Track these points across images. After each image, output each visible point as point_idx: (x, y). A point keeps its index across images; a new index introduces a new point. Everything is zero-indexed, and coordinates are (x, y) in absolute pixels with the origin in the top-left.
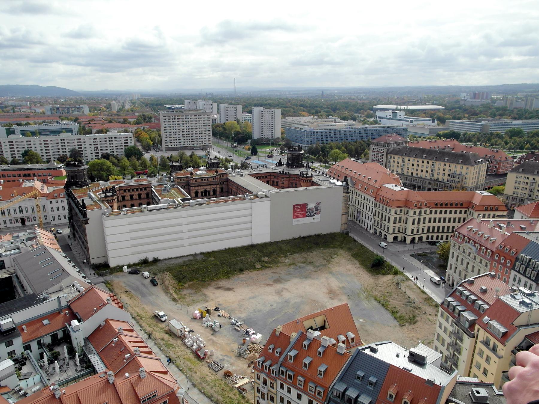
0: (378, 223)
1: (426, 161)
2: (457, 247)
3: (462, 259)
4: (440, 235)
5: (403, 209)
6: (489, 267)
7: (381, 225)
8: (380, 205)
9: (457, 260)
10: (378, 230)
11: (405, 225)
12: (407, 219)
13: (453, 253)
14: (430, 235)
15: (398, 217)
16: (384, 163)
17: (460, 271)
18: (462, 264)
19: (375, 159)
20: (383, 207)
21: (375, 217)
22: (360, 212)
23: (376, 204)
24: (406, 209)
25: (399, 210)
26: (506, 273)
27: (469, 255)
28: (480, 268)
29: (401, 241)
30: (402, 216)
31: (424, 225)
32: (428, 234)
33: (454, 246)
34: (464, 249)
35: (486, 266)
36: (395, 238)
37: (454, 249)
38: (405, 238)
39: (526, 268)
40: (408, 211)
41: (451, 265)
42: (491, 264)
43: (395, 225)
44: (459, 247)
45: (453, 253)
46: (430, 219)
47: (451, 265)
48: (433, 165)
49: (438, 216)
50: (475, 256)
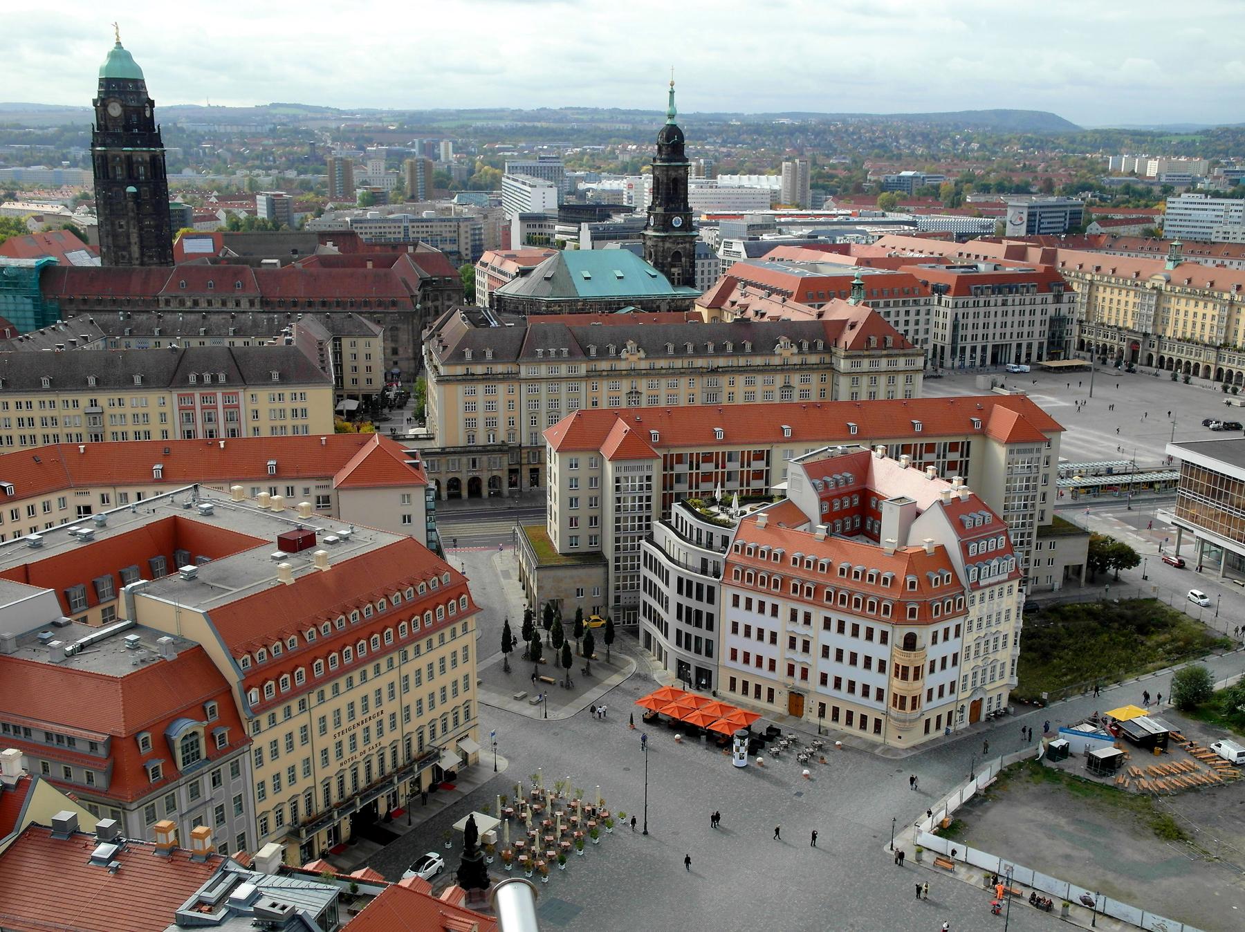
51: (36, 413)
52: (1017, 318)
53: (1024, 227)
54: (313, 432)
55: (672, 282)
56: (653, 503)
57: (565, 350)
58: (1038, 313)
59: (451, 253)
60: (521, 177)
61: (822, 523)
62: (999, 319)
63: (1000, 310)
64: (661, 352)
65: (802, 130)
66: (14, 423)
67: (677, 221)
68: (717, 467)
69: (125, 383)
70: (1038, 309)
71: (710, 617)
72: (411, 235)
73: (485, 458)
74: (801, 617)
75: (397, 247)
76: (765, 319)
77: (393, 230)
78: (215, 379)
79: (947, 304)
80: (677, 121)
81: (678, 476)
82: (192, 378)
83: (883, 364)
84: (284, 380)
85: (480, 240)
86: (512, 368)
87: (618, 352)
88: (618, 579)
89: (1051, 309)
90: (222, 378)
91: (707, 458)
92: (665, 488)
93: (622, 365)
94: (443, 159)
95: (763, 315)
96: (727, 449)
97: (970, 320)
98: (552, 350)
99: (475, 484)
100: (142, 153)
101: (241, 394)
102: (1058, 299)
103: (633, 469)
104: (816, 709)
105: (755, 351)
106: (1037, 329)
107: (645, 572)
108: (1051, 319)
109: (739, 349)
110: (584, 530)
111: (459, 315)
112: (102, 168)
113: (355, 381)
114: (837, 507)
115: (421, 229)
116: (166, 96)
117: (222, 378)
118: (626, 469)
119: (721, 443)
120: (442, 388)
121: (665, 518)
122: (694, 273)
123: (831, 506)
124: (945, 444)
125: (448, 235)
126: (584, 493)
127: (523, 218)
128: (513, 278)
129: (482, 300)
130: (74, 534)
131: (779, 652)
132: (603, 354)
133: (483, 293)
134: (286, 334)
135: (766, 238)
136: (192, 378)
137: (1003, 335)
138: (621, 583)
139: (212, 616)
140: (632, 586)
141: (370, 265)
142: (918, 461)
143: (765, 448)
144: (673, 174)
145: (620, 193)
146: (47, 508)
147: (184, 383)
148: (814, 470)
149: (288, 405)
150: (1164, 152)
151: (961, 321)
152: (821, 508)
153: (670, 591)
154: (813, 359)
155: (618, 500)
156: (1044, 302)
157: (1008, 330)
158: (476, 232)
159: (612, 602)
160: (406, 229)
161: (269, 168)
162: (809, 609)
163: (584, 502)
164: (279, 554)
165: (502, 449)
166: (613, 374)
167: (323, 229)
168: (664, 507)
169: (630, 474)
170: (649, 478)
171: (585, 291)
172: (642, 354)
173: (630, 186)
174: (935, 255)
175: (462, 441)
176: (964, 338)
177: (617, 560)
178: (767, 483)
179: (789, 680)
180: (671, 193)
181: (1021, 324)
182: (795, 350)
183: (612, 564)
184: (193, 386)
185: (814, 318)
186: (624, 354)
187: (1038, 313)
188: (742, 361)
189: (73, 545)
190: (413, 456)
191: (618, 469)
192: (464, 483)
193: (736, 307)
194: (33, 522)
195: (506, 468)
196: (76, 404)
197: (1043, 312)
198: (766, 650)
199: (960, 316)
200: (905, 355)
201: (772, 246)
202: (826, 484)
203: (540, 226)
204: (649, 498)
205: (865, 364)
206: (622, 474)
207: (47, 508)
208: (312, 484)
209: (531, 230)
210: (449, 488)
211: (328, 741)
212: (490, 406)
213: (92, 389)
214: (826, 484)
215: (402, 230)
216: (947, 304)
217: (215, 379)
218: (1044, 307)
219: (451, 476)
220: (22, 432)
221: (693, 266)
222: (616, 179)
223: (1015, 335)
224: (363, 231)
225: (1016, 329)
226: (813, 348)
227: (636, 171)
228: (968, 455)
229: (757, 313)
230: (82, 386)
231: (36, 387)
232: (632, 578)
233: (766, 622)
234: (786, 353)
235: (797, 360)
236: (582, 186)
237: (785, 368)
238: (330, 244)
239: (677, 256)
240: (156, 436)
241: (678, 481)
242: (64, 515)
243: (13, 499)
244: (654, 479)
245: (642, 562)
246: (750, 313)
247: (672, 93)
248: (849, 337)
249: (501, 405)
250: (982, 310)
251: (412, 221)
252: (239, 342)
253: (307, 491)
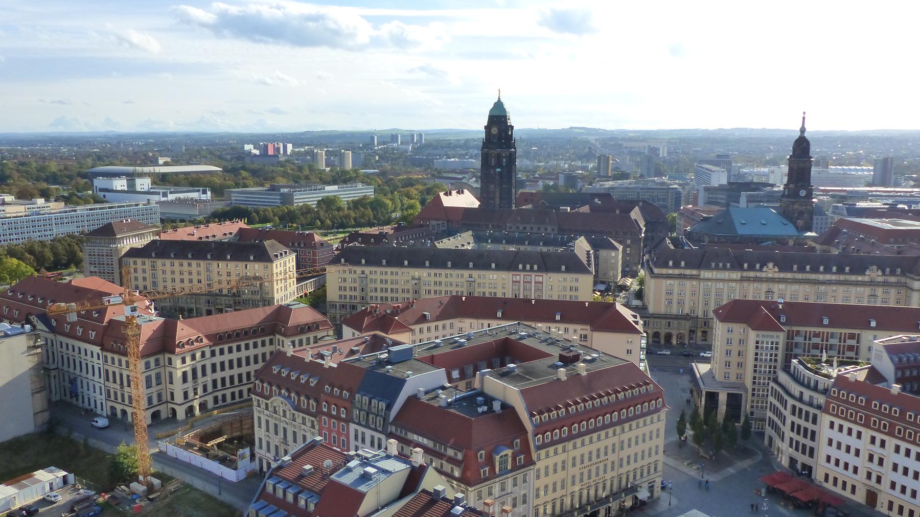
0: (116, 393)
1: (194, 263)
2: (263, 406)
3: (276, 426)
4: (236, 390)
5: (160, 356)
6: (317, 427)
7: (123, 396)
8: (113, 359)
9: (268, 430)
10: (119, 407)
11: (169, 386)
12: (171, 374)
13: (259, 418)
14: (219, 394)
15: (153, 374)
16: (117, 276)
17: (277, 447)
18: (276, 433)
19: (96, 270)
20: (120, 361)
21: (107, 383)
22: (75, 379)
23: (106, 357)
24: (167, 356)
25: (152, 360)
26: (343, 429)
27: (285, 416)
28: (304, 433)
29: (168, 418)
30: (161, 370)
31: (205, 379)
32: (216, 394)
33: (259, 406)
34: (275, 407)
35: (313, 427)
36: (155, 416)
37: (259, 411)
38: (174, 411)
39: (368, 414)
40: (170, 360)
41: (260, 440)
42: (320, 422)
43: (150, 390)
44: (267, 404)
45: (259, 418)
46: (214, 366)
47: (260, 440)
48: (208, 270)
49: (226, 357)
50: (294, 415)
51: (443, 279)
54: (580, 300)
55: (797, 228)
56: (779, 358)
57: (728, 265)
61: (897, 383)
64: (790, 270)
66: (433, 284)
67: (803, 193)
69: (487, 267)
71: (813, 433)
73: (676, 322)
74: (878, 442)
78: (532, 268)
80: (806, 135)
81: (797, 344)
82: (520, 266)
84: (568, 271)
86: (694, 272)
87: (761, 267)
88: (753, 401)
90: (536, 267)
91: (817, 335)
92: (787, 350)
93: (763, 275)
96: (831, 330)
98: (721, 265)
103: (768, 336)
104: (886, 505)
105: (852, 272)
107: (771, 399)
109: (841, 271)
110: (734, 370)
114: (908, 373)
116: (519, 122)
117: (536, 267)
118: (763, 336)
119: (826, 326)
121: (786, 368)
122: (812, 223)
123: (903, 373)
126: (735, 348)
127: (707, 189)
131: (862, 462)
132: (752, 268)
136: (520, 266)
139: (523, 393)
140: (762, 407)
141: (618, 212)
143: (856, 332)
144: (802, 165)
146: (444, 327)
147: (516, 269)
148: (891, 350)
149: (568, 284)
152: (896, 374)
153: (787, 413)
154: (893, 279)
160: (638, 193)
162: (885, 437)
163: (735, 353)
165: (686, 317)
166: (757, 280)
168: (786, 361)
169: (765, 340)
170: (777, 343)
171: (742, 231)
172: (776, 269)
175: (663, 311)
177: (754, 390)
178: (857, 354)
179: (868, 482)
182: (880, 273)
183: (750, 392)
184: (520, 271)
186: (765, 269)
188: (842, 277)
191: (758, 336)
194: (437, 334)
195: (688, 328)
196: (462, 276)
198: (851, 459)
202: (900, 360)
204: (776, 355)
206: (760, 339)
207: (444, 327)
208: (578, 327)
210: (653, 337)
211: (576, 471)
213: (471, 269)
214: (900, 360)
217: (532, 268)
219: (655, 330)
220: (436, 288)
221: (811, 219)
226: (893, 273)
230: (466, 267)
231: (444, 266)
232: (762, 402)
233: (853, 442)
234: (873, 275)
235: (880, 279)
237: (872, 283)
240: (499, 295)
241: (796, 347)
242: (452, 331)
243: (429, 321)
245: (769, 393)
247: (804, 118)
252: (545, 249)
253: (575, 331)
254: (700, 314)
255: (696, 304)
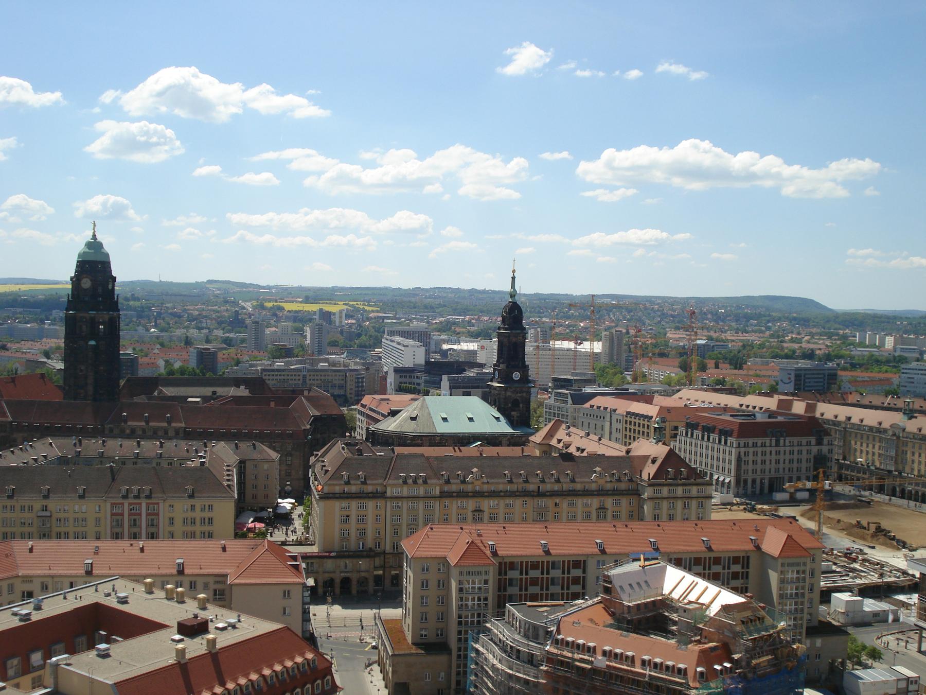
52: (788, 457)
53: (792, 384)
58: (804, 453)
59: (339, 396)
60: (398, 338)
62: (774, 457)
63: (774, 449)
65: (618, 307)
67: (516, 376)
68: (542, 573)
70: (804, 449)
72: (308, 382)
75: (296, 392)
76: (585, 454)
77: (294, 378)
79: (732, 444)
81: (511, 580)
83: (680, 491)
85: (362, 386)
89: (815, 449)
94: (337, 324)
95: (583, 450)
97: (751, 458)
99: (346, 581)
100: (105, 316)
101: (161, 505)
102: (819, 443)
103: (474, 573)
106: (804, 465)
108: (815, 457)
111: (340, 444)
112: (71, 325)
113: (254, 497)
115: (316, 378)
120: (322, 503)
124: (729, 558)
125: (337, 382)
127: (397, 370)
128: (385, 416)
129: (360, 434)
130: (15, 614)
133: (362, 428)
134: (201, 457)
135: (588, 390)
137: (777, 470)
138: (461, 670)
142: (707, 572)
145: (474, 353)
150: (898, 330)
151: (744, 458)
155: (461, 599)
156: (809, 444)
157: (781, 466)
158: (359, 381)
159: (453, 686)
161: (203, 328)
164: (178, 637)
167: (240, 375)
168: (499, 606)
171: (442, 428)
173: (482, 348)
174: (722, 405)
176: (746, 472)
180: (512, 352)
181: (791, 461)
185: (624, 454)
187: (804, 453)
189: (16, 622)
190: (294, 558)
192: (338, 581)
193: (561, 444)
197: (809, 452)
199: (742, 454)
200: (697, 484)
201: (593, 396)
203: (410, 377)
204: (486, 599)
205: (665, 491)
209: (403, 380)
212: (361, 520)
215: (301, 378)
216: (732, 444)
218: (809, 448)
222: (472, 342)
223: (787, 470)
224: (271, 378)
225: (787, 465)
227: (488, 337)
228: (748, 567)
229: (578, 449)
236: (445, 347)
237: (601, 493)
238: (242, 387)
239: (516, 403)
241: (511, 584)
244: (491, 582)
246: (572, 450)
247: (513, 278)
248: (650, 470)
249: (370, 519)
250: (760, 450)
251: (309, 371)
254: (388, 548)
255: (382, 533)
